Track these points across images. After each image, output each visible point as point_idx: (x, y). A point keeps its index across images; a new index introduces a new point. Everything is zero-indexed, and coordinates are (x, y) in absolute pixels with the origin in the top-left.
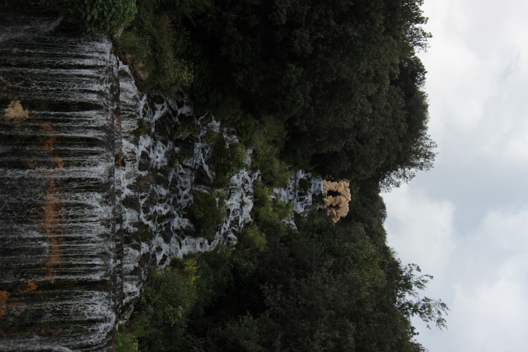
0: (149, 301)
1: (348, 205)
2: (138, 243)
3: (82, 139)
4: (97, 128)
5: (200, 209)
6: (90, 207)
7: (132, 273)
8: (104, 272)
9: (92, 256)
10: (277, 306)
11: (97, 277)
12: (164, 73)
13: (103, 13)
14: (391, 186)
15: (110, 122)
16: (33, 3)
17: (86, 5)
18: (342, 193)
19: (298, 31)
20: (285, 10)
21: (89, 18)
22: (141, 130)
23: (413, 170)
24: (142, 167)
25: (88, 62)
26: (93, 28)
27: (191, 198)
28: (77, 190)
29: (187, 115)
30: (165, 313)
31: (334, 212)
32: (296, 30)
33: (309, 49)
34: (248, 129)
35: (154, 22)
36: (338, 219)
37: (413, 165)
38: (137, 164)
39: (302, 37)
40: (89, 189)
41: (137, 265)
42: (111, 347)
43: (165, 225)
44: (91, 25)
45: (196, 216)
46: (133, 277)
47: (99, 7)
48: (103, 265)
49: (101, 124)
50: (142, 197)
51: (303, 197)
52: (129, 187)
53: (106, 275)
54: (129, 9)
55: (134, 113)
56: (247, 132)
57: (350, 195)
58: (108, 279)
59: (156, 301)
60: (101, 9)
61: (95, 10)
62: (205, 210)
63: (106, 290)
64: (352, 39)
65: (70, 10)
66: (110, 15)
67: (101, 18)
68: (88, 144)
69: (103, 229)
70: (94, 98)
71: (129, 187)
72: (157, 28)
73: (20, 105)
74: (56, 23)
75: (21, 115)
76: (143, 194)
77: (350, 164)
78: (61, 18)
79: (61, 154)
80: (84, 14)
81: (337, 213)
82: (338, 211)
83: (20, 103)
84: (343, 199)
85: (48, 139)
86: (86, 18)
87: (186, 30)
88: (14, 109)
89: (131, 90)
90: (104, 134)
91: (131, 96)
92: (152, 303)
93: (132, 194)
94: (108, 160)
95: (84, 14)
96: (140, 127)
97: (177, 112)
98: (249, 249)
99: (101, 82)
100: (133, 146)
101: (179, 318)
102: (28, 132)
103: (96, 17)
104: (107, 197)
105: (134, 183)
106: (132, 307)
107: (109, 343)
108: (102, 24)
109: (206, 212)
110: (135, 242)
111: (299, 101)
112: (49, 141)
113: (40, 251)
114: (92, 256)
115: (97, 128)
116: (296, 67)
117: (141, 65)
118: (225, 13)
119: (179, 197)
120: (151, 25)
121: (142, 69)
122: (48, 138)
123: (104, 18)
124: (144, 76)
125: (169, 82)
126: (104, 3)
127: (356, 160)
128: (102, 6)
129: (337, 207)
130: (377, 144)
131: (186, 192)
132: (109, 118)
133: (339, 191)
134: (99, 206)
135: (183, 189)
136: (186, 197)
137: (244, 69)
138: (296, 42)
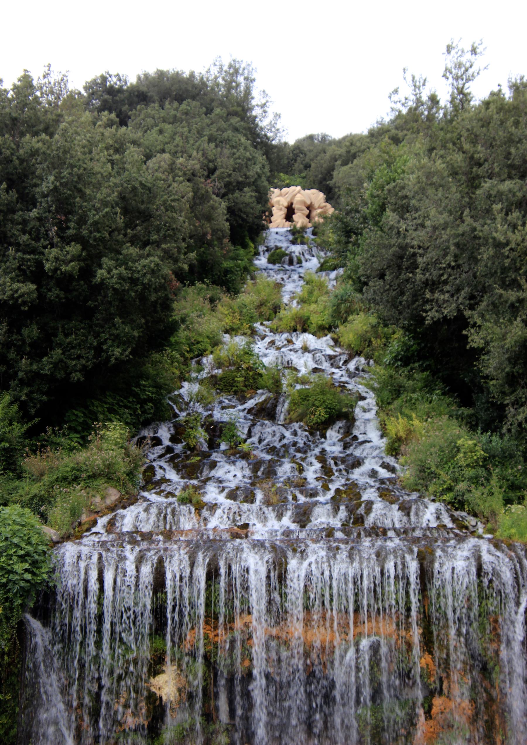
0: (450, 489)
1: (307, 191)
2: (363, 505)
3: (208, 587)
4: (192, 565)
5: (313, 413)
6: (308, 577)
7: (408, 515)
8: (406, 555)
9: (382, 573)
10: (458, 298)
11: (413, 566)
12: (109, 466)
13: (19, 556)
14: (278, 127)
15: (184, 545)
16: (6, 658)
17: (9, 581)
18: (289, 199)
19: (47, 266)
20: (16, 286)
21: (28, 576)
22: (194, 501)
23: (255, 93)
24: (250, 499)
26: (43, 570)
28: (283, 595)
29: (172, 431)
30: (468, 466)
32: (46, 268)
33: (74, 249)
34: (193, 340)
35: (34, 480)
36: (328, 205)
37: (248, 92)
38: (246, 506)
39: (57, 259)
40: (282, 578)
41: (395, 507)
43: (336, 464)
44: (38, 572)
45: (323, 419)
46: (412, 514)
47: (11, 562)
48: (396, 557)
50: (295, 498)
51: (295, 259)
52: (279, 517)
53: (411, 551)
54: (14, 518)
55: (169, 510)
56: (198, 342)
57: (292, 188)
58: (416, 550)
60: (15, 559)
61: (16, 567)
62: (314, 405)
63: (432, 553)
64: (58, 184)
65: (16, 604)
66: (23, 545)
67: (27, 558)
68: (216, 578)
69: (343, 555)
70: (147, 570)
71: (279, 517)
72: (42, 475)
73: (157, 678)
74: (35, 624)
76: (290, 498)
77: (246, 189)
78: (28, 616)
79: (231, 619)
80: (22, 584)
81: (319, 207)
82: (316, 205)
83: (154, 677)
84: (298, 198)
85: (208, 637)
86: (28, 581)
87: (45, 432)
89: (134, 514)
90: (200, 556)
91: (143, 515)
92: (452, 484)
93: (289, 513)
94: (239, 550)
95: (22, 584)
96: (191, 502)
97: (168, 447)
98: (373, 339)
99: (122, 558)
100: (219, 512)
101: (475, 445)
102: (200, 665)
103: (26, 566)
104: (295, 551)
105: (274, 510)
106: (457, 514)
107: (511, 547)
108: (37, 557)
109: (317, 403)
110: (361, 510)
111: (152, 265)
112: (211, 635)
113: (375, 648)
115: (192, 565)
116: (101, 267)
117: (98, 500)
118: (21, 375)
119: (295, 444)
120: (38, 485)
121: (103, 498)
122: (206, 637)
123: (28, 554)
124: (113, 495)
125: (123, 459)
126: (5, 554)
127: (240, 179)
128: (10, 557)
129: (310, 207)
130: (216, 146)
131: (287, 434)
132: (176, 547)
133: (286, 204)
134: (306, 564)
135: (283, 437)
136: (295, 434)
137: (105, 347)
138: (63, 268)
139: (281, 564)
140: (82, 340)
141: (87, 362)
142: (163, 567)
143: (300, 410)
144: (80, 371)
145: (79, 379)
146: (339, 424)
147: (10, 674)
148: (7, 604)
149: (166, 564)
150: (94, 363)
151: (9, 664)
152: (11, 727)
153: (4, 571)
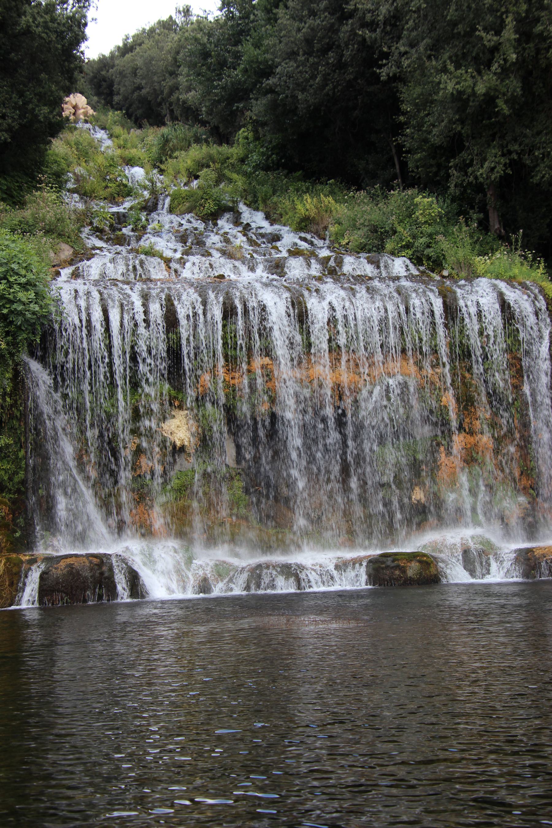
4: (204, 303)
7: (378, 267)
9: (407, 310)
11: (438, 304)
16: (8, 399)
25: (97, 315)
27: (188, 216)
30: (426, 222)
31: (82, 111)
36: (89, 108)
42: (528, 282)
46: (382, 265)
49: (195, 296)
52: (252, 269)
59: (410, 236)
62: (202, 198)
66: (23, 272)
71: (252, 269)
73: (166, 423)
74: (35, 366)
75: (184, 421)
81: (83, 108)
82: (80, 106)
88: (176, 431)
92: (411, 240)
114: (407, 310)
123: (28, 283)
128: (10, 285)
135: (181, 225)
137: (30, 106)
139: (300, 303)
140: (6, 99)
141: (13, 122)
142: (173, 305)
143: (188, 205)
144: (6, 131)
145: (6, 139)
146: (227, 216)
147: (12, 417)
148: (10, 338)
149: (176, 303)
150: (20, 124)
151: (12, 406)
152: (16, 473)
153: (4, 301)
